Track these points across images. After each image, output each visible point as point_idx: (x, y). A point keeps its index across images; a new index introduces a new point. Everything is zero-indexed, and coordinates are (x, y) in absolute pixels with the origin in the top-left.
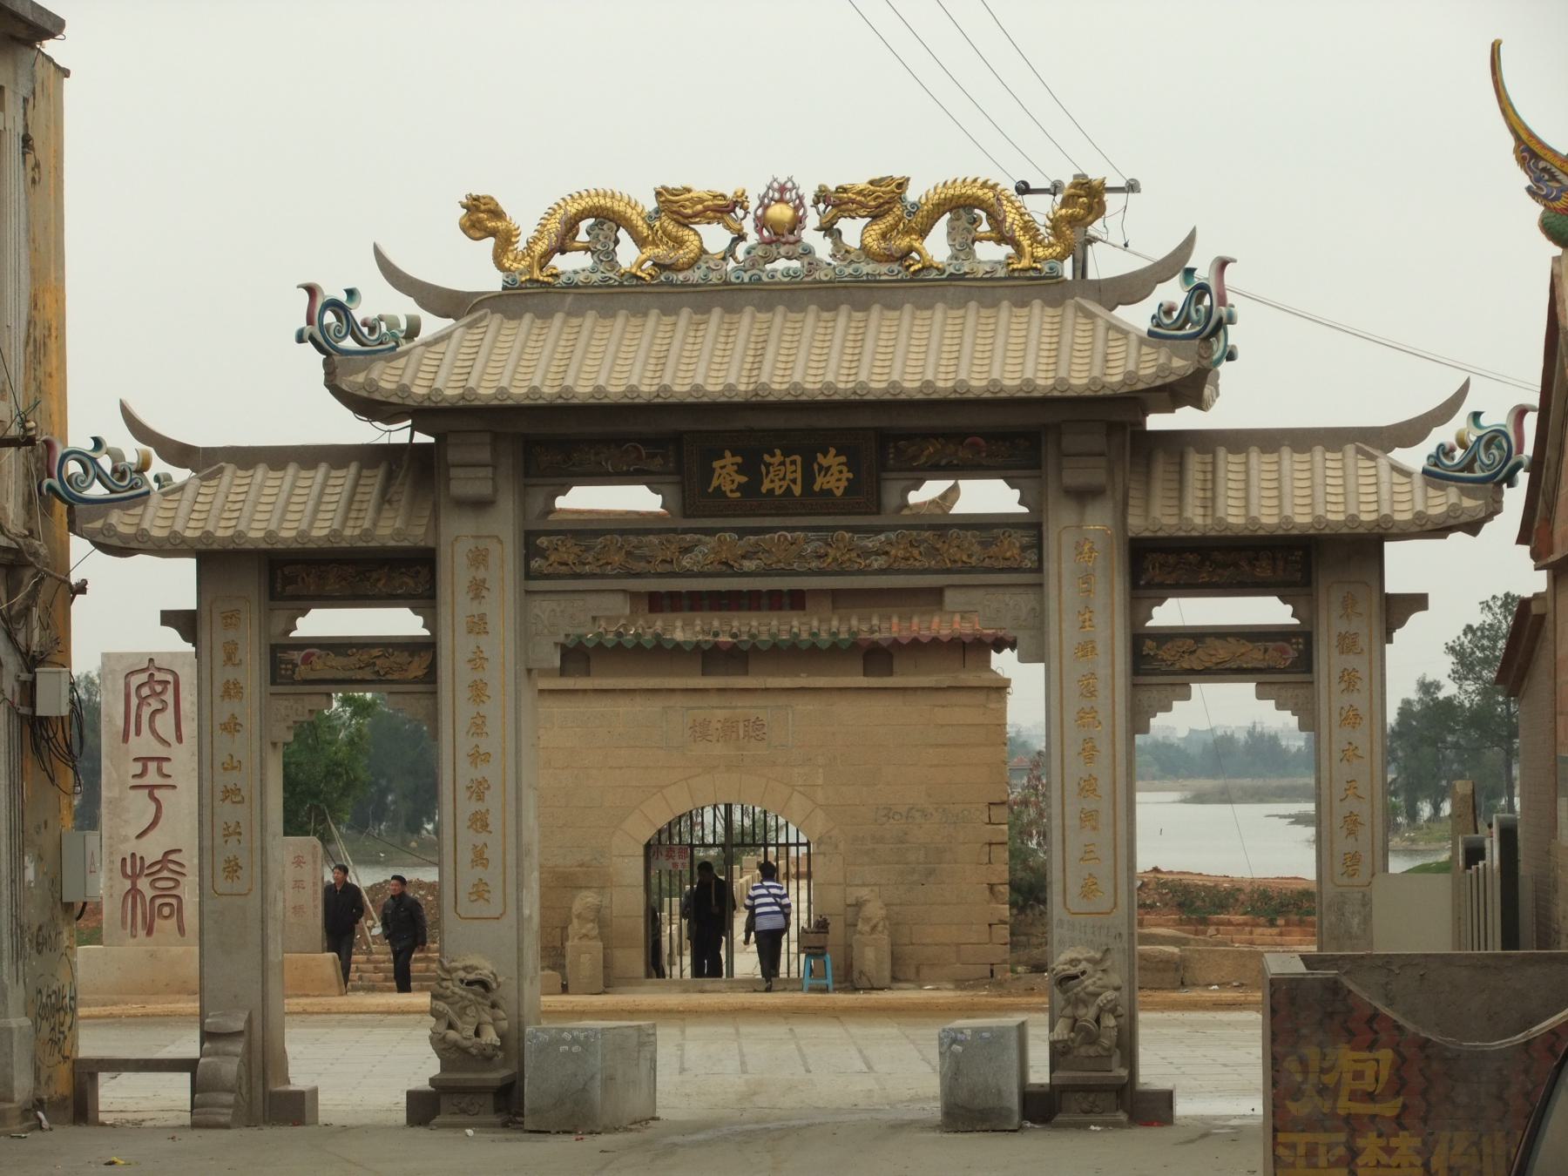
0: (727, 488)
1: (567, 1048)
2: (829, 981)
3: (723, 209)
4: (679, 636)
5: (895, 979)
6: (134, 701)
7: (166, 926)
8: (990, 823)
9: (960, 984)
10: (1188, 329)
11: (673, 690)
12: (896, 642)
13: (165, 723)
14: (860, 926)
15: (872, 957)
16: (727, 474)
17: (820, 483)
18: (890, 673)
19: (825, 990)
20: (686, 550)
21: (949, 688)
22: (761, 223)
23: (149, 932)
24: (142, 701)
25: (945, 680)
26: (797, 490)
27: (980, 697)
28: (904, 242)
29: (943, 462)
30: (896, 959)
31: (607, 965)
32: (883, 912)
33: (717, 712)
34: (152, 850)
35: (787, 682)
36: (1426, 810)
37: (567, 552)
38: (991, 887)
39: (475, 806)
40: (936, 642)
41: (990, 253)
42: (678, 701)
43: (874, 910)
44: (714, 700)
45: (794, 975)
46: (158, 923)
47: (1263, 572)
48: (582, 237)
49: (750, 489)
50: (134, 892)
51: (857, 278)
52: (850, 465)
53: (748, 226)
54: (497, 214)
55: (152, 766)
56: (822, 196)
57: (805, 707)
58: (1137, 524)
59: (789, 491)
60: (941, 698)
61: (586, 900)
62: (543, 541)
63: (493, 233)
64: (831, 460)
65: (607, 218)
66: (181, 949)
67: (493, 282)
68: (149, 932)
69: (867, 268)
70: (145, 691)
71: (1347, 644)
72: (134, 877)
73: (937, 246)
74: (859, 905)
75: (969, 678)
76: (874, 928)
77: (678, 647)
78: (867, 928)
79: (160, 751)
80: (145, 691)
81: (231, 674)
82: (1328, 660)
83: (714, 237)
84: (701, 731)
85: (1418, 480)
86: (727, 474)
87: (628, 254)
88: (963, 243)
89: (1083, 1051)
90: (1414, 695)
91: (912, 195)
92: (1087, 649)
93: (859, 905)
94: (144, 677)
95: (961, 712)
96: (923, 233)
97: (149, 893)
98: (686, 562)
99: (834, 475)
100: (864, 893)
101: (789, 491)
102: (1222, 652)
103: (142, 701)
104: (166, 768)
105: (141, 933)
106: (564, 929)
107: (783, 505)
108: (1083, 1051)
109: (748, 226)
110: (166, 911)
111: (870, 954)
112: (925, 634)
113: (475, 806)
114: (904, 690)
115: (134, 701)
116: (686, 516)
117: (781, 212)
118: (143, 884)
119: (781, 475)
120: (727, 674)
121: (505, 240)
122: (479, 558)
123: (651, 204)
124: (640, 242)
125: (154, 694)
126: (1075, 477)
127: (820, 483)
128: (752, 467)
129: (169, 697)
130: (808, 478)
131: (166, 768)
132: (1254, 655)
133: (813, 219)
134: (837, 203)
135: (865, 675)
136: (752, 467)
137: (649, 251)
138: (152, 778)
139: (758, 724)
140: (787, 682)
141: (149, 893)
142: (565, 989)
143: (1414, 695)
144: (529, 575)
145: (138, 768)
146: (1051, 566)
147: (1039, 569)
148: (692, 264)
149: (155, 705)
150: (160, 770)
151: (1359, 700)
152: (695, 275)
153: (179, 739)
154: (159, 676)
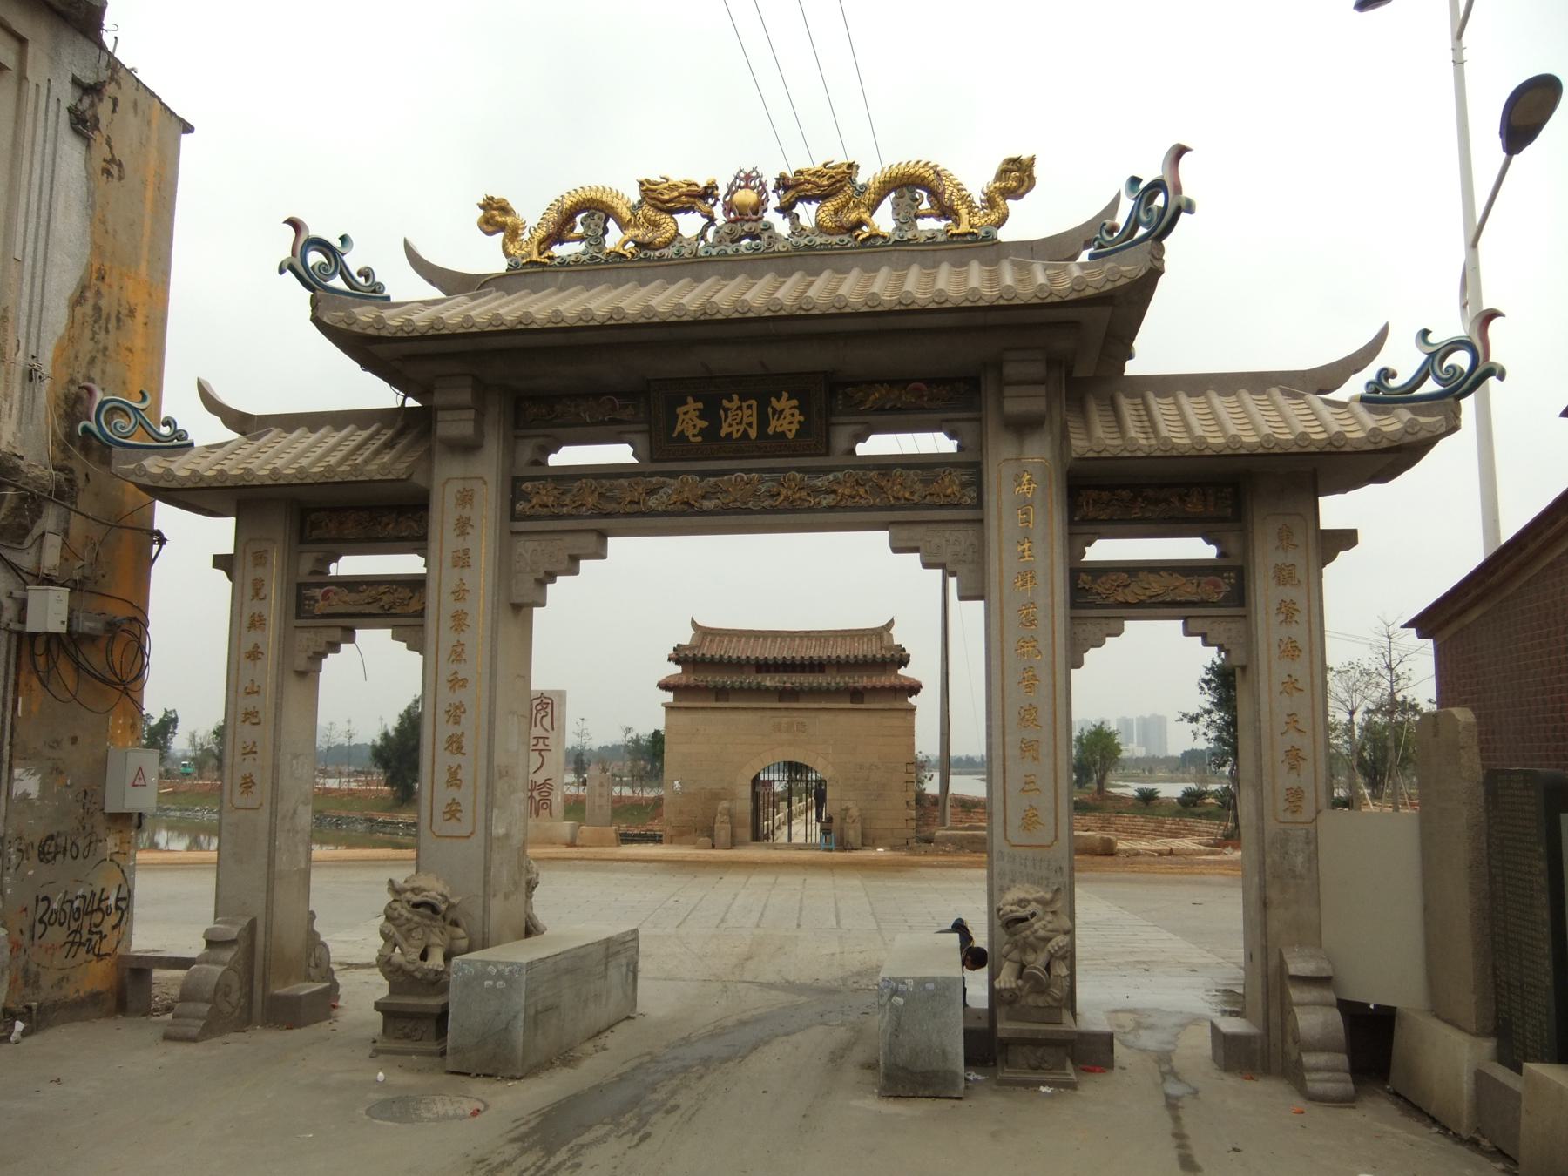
0: (689, 432)
2: (833, 846)
3: (699, 196)
4: (768, 683)
5: (863, 845)
6: (534, 712)
7: (544, 813)
8: (907, 772)
9: (893, 848)
10: (1142, 231)
11: (764, 709)
12: (865, 688)
13: (547, 721)
14: (848, 820)
15: (853, 834)
16: (689, 421)
17: (774, 426)
18: (862, 702)
19: (830, 850)
20: (651, 492)
21: (890, 710)
22: (729, 208)
23: (537, 816)
24: (538, 711)
25: (888, 706)
26: (753, 433)
27: (903, 714)
28: (853, 216)
29: (888, 406)
30: (864, 836)
31: (733, 835)
32: (857, 814)
33: (785, 719)
34: (539, 778)
35: (816, 706)
37: (547, 495)
38: (907, 802)
40: (883, 688)
41: (928, 225)
42: (769, 713)
43: (854, 812)
44: (783, 713)
45: (814, 841)
46: (541, 812)
47: (1194, 507)
48: (579, 229)
49: (710, 434)
50: (531, 797)
51: (810, 247)
52: (802, 408)
53: (718, 211)
54: (505, 209)
55: (541, 741)
56: (783, 183)
57: (825, 717)
58: (1080, 445)
59: (745, 434)
61: (724, 805)
62: (527, 486)
63: (502, 227)
64: (785, 403)
65: (596, 209)
66: (548, 824)
67: (500, 265)
68: (537, 816)
69: (818, 240)
70: (539, 707)
71: (1284, 575)
72: (532, 790)
73: (884, 220)
74: (847, 810)
75: (898, 705)
76: (853, 822)
77: (767, 689)
78: (850, 821)
79: (545, 735)
80: (539, 707)
81: (257, 607)
82: (1265, 592)
83: (689, 224)
84: (777, 728)
85: (1359, 409)
86: (689, 421)
87: (614, 238)
88: (907, 216)
91: (861, 178)
92: (1027, 576)
93: (847, 810)
94: (539, 701)
95: (894, 721)
96: (873, 208)
97: (538, 798)
98: (652, 502)
99: (787, 418)
100: (850, 804)
101: (745, 434)
102: (1156, 585)
103: (538, 711)
104: (547, 742)
105: (534, 816)
106: (714, 818)
107: (740, 448)
109: (718, 211)
110: (545, 806)
111: (851, 832)
112: (878, 684)
115: (534, 712)
116: (653, 460)
117: (747, 197)
118: (535, 794)
119: (739, 419)
120: (790, 701)
121: (513, 233)
122: (466, 498)
123: (635, 196)
124: (623, 226)
125: (543, 709)
126: (1016, 404)
127: (774, 426)
128: (711, 412)
129: (549, 710)
130: (763, 422)
131: (547, 742)
132: (1188, 589)
133: (774, 201)
134: (794, 189)
135: (852, 702)
136: (711, 412)
137: (631, 232)
138: (541, 746)
139: (803, 725)
140: (816, 706)
141: (538, 798)
142: (713, 847)
144: (514, 517)
145: (535, 742)
146: (991, 499)
147: (979, 503)
148: (667, 244)
149: (543, 713)
150: (544, 743)
151: (1298, 632)
152: (669, 252)
153: (553, 729)
154: (545, 701)
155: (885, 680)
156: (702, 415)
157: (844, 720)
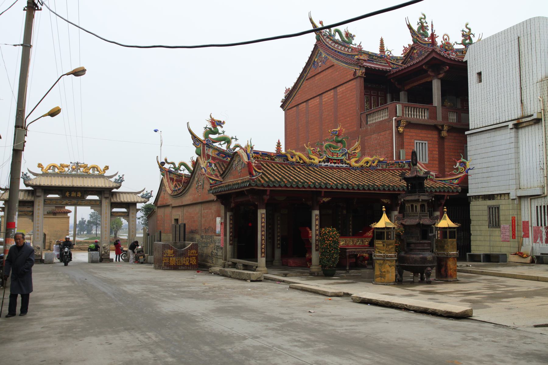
1: (351, 226)
10: (119, 181)
17: (78, 195)
20: (62, 202)
22: (72, 168)
26: (75, 196)
27: (66, 219)
28: (87, 171)
36: (82, 233)
37: (49, 202)
39: (37, 229)
41: (96, 173)
47: (124, 206)
48: (51, 168)
49: (70, 196)
51: (82, 174)
53: (70, 168)
54: (42, 165)
58: (112, 201)
60: (62, 218)
62: (46, 201)
63: (41, 167)
65: (54, 166)
67: (41, 173)
69: (83, 173)
71: (133, 213)
73: (91, 171)
74: (51, 241)
82: (131, 215)
83: (66, 169)
85: (141, 197)
86: (67, 194)
88: (94, 171)
89: (106, 254)
90: (81, 220)
91: (88, 166)
92: (106, 213)
93: (51, 241)
95: (65, 220)
96: (89, 170)
98: (62, 203)
99: (79, 194)
100: (52, 240)
102: (120, 214)
107: (73, 198)
108: (106, 254)
109: (70, 168)
113: (37, 229)
114: (57, 217)
119: (74, 194)
121: (42, 168)
122: (39, 202)
123: (59, 165)
124: (58, 169)
126: (106, 196)
127: (78, 195)
128: (70, 194)
132: (123, 214)
136: (70, 194)
137: (59, 170)
143: (81, 220)
144: (44, 204)
146: (102, 205)
147: (101, 205)
148: (64, 172)
151: (134, 219)
152: (64, 173)
155: (62, 210)
156: (69, 194)
157: (51, 220)
